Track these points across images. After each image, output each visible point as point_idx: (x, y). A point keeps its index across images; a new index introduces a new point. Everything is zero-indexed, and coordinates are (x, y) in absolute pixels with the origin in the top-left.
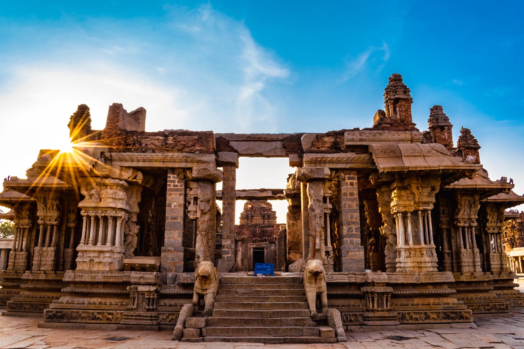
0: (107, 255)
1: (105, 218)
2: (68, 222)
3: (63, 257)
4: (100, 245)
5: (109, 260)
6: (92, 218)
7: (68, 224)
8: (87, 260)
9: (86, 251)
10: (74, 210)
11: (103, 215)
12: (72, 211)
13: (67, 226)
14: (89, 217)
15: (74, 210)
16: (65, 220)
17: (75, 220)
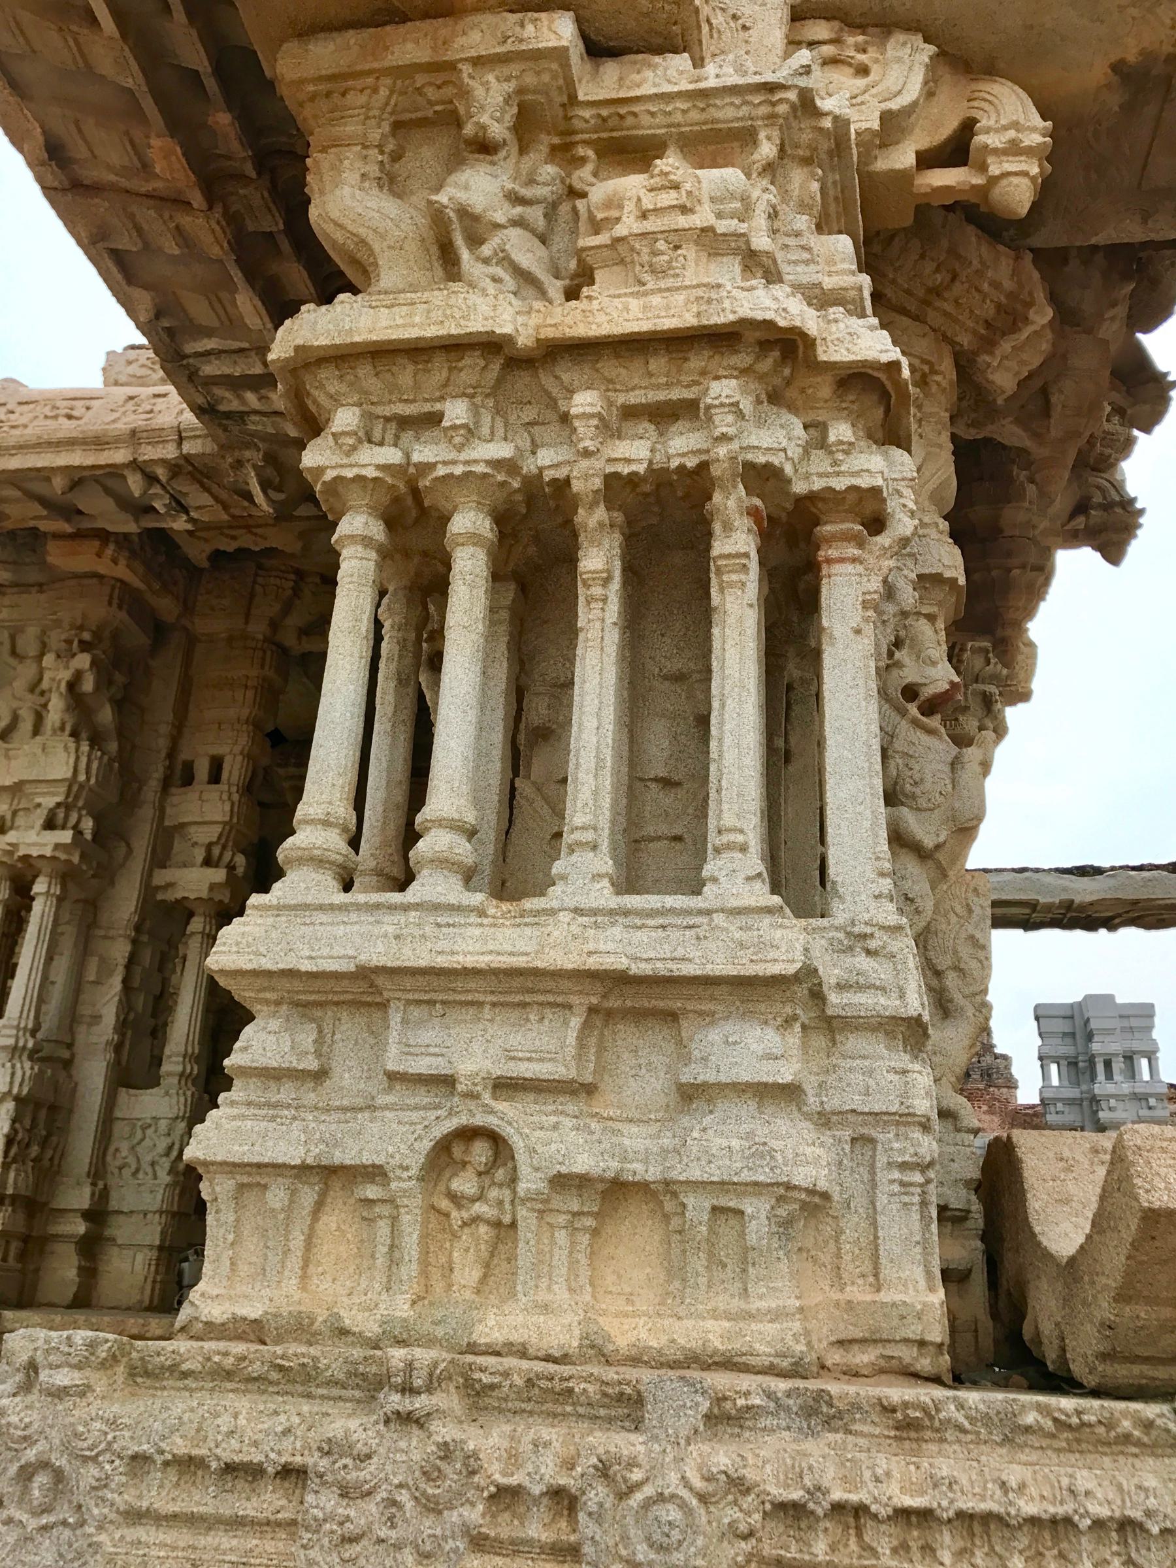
0: (752, 1048)
1: (666, 525)
2: (161, 857)
3: (98, 1172)
4: (603, 896)
5: (804, 1155)
6: (469, 523)
7: (161, 877)
8: (396, 1138)
9: (365, 992)
10: (217, 765)
11: (635, 452)
12: (202, 770)
13: (149, 891)
14: (414, 518)
15: (217, 765)
16: (141, 844)
17: (223, 841)
